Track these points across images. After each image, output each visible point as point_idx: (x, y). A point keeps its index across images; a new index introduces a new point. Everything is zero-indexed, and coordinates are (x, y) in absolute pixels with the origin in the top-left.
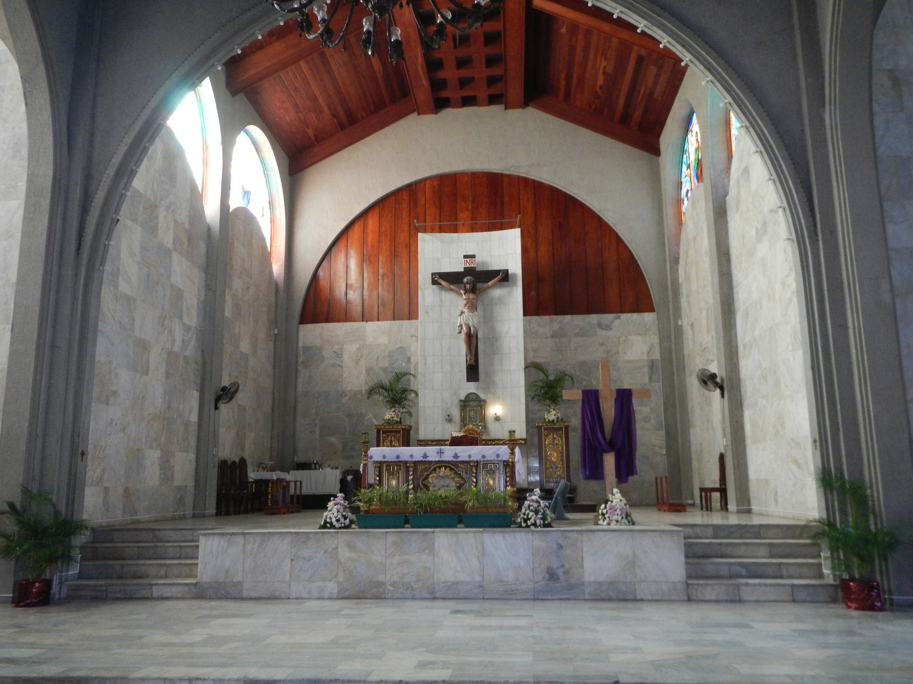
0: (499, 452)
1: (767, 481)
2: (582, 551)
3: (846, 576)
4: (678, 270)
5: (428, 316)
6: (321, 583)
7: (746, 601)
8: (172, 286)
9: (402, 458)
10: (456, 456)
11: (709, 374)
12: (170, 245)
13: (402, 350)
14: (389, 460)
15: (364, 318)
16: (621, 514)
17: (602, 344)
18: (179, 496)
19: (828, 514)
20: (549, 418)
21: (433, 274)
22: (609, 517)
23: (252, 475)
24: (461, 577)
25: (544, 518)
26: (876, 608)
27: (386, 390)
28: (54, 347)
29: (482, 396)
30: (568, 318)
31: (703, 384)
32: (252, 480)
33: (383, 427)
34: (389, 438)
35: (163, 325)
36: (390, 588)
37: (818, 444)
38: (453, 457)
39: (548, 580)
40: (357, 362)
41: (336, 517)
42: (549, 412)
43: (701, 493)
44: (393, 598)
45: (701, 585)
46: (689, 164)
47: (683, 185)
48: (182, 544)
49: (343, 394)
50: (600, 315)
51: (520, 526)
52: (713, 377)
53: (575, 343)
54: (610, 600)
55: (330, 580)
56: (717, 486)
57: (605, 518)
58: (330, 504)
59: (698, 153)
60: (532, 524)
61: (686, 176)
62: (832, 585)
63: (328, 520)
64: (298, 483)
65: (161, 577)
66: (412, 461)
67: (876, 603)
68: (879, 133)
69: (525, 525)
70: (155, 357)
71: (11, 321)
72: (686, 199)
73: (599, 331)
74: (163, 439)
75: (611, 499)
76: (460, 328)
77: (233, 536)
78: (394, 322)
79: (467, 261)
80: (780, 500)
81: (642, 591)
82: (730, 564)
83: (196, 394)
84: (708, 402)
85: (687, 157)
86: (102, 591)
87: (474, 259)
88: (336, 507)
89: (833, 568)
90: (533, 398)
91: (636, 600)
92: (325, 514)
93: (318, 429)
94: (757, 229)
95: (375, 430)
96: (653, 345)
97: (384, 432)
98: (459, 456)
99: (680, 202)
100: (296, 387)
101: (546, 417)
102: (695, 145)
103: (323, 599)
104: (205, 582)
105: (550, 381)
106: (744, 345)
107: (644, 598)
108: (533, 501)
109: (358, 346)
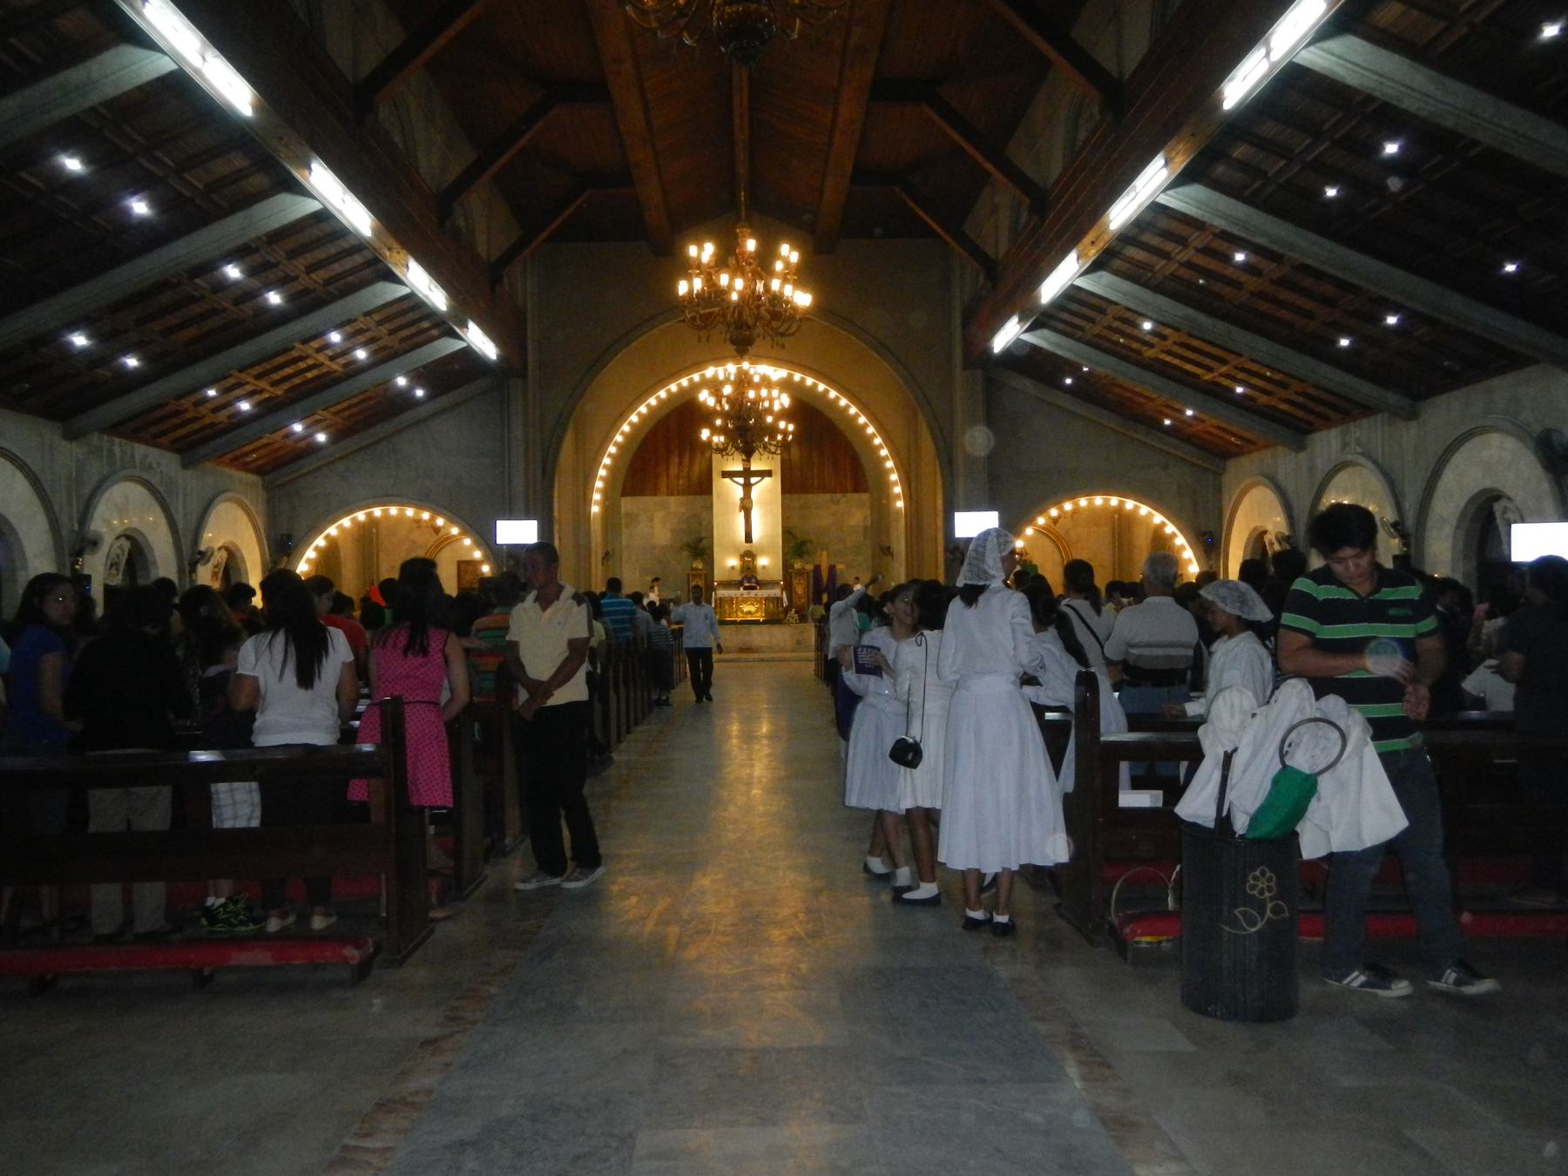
15: (670, 493)
30: (810, 496)
49: (655, 547)
52: (889, 548)
69: (789, 623)
93: (637, 572)
100: (621, 542)
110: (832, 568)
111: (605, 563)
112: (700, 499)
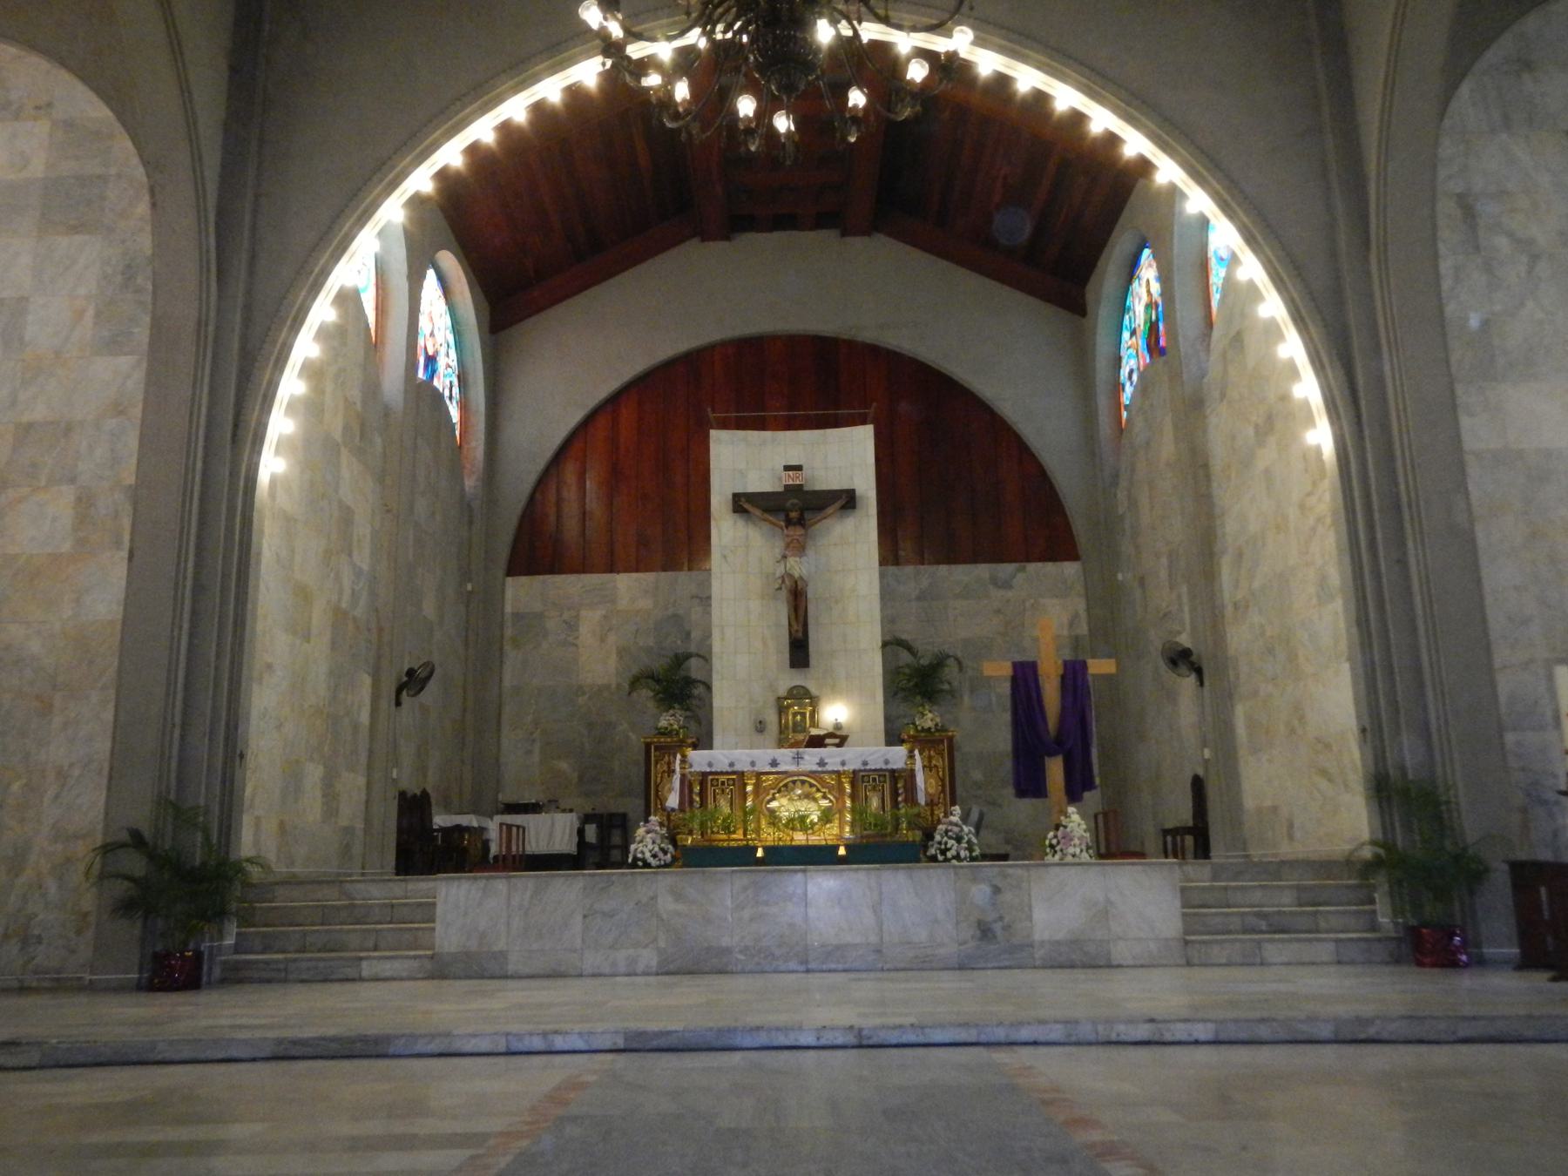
0: (888, 757)
1: (1275, 809)
2: (1029, 895)
3: (1413, 922)
4: (1115, 496)
5: (727, 561)
6: (631, 951)
7: (1270, 965)
8: (340, 502)
9: (738, 768)
10: (822, 763)
11: (1180, 649)
12: (338, 435)
13: (677, 620)
14: (719, 770)
15: (611, 568)
16: (1080, 844)
17: (998, 611)
18: (345, 842)
19: (1385, 833)
20: (923, 724)
21: (736, 497)
22: (1061, 850)
23: (440, 820)
24: (849, 938)
25: (970, 849)
26: (1461, 964)
27: (658, 681)
28: (199, 589)
29: (814, 690)
30: (943, 569)
31: (1171, 666)
32: (437, 827)
33: (655, 740)
34: (667, 757)
35: (328, 565)
36: (741, 957)
37: (1369, 735)
38: (818, 764)
39: (981, 939)
40: (603, 640)
41: (650, 851)
42: (923, 715)
43: (1165, 837)
44: (743, 972)
45: (1204, 942)
46: (1135, 330)
47: (1124, 362)
48: (394, 901)
49: (580, 690)
50: (993, 566)
51: (933, 859)
53: (955, 609)
54: (1072, 966)
55: (646, 946)
56: (1190, 823)
57: (1056, 852)
58: (641, 831)
59: (1149, 312)
60: (954, 858)
61: (1129, 348)
62: (1394, 939)
63: (639, 855)
64: (521, 830)
65: (368, 950)
66: (753, 772)
67: (1459, 957)
68: (1446, 284)
69: (941, 858)
70: (319, 617)
71: (127, 544)
72: (1128, 385)
73: (991, 587)
74: (326, 749)
75: (1064, 823)
76: (780, 581)
77: (491, 881)
78: (663, 574)
79: (789, 476)
80: (1298, 835)
81: (1120, 952)
82: (1243, 914)
83: (367, 680)
84: (1171, 696)
85: (1130, 318)
86: (279, 970)
87: (800, 472)
88: (650, 835)
89: (1397, 911)
90: (896, 694)
91: (1110, 966)
92: (633, 847)
94: (1257, 426)
95: (643, 746)
96: (1076, 616)
97: (657, 749)
98: (826, 764)
99: (1118, 388)
100: (501, 680)
101: (917, 723)
102: (1145, 298)
103: (636, 975)
104: (447, 953)
105: (923, 666)
106: (1235, 604)
107: (1125, 963)
108: (951, 823)
109: (604, 612)
110: (1074, 675)
111: (404, 693)
112: (683, 580)
